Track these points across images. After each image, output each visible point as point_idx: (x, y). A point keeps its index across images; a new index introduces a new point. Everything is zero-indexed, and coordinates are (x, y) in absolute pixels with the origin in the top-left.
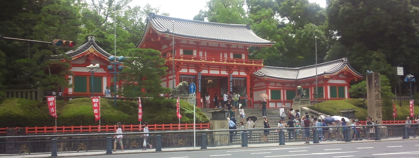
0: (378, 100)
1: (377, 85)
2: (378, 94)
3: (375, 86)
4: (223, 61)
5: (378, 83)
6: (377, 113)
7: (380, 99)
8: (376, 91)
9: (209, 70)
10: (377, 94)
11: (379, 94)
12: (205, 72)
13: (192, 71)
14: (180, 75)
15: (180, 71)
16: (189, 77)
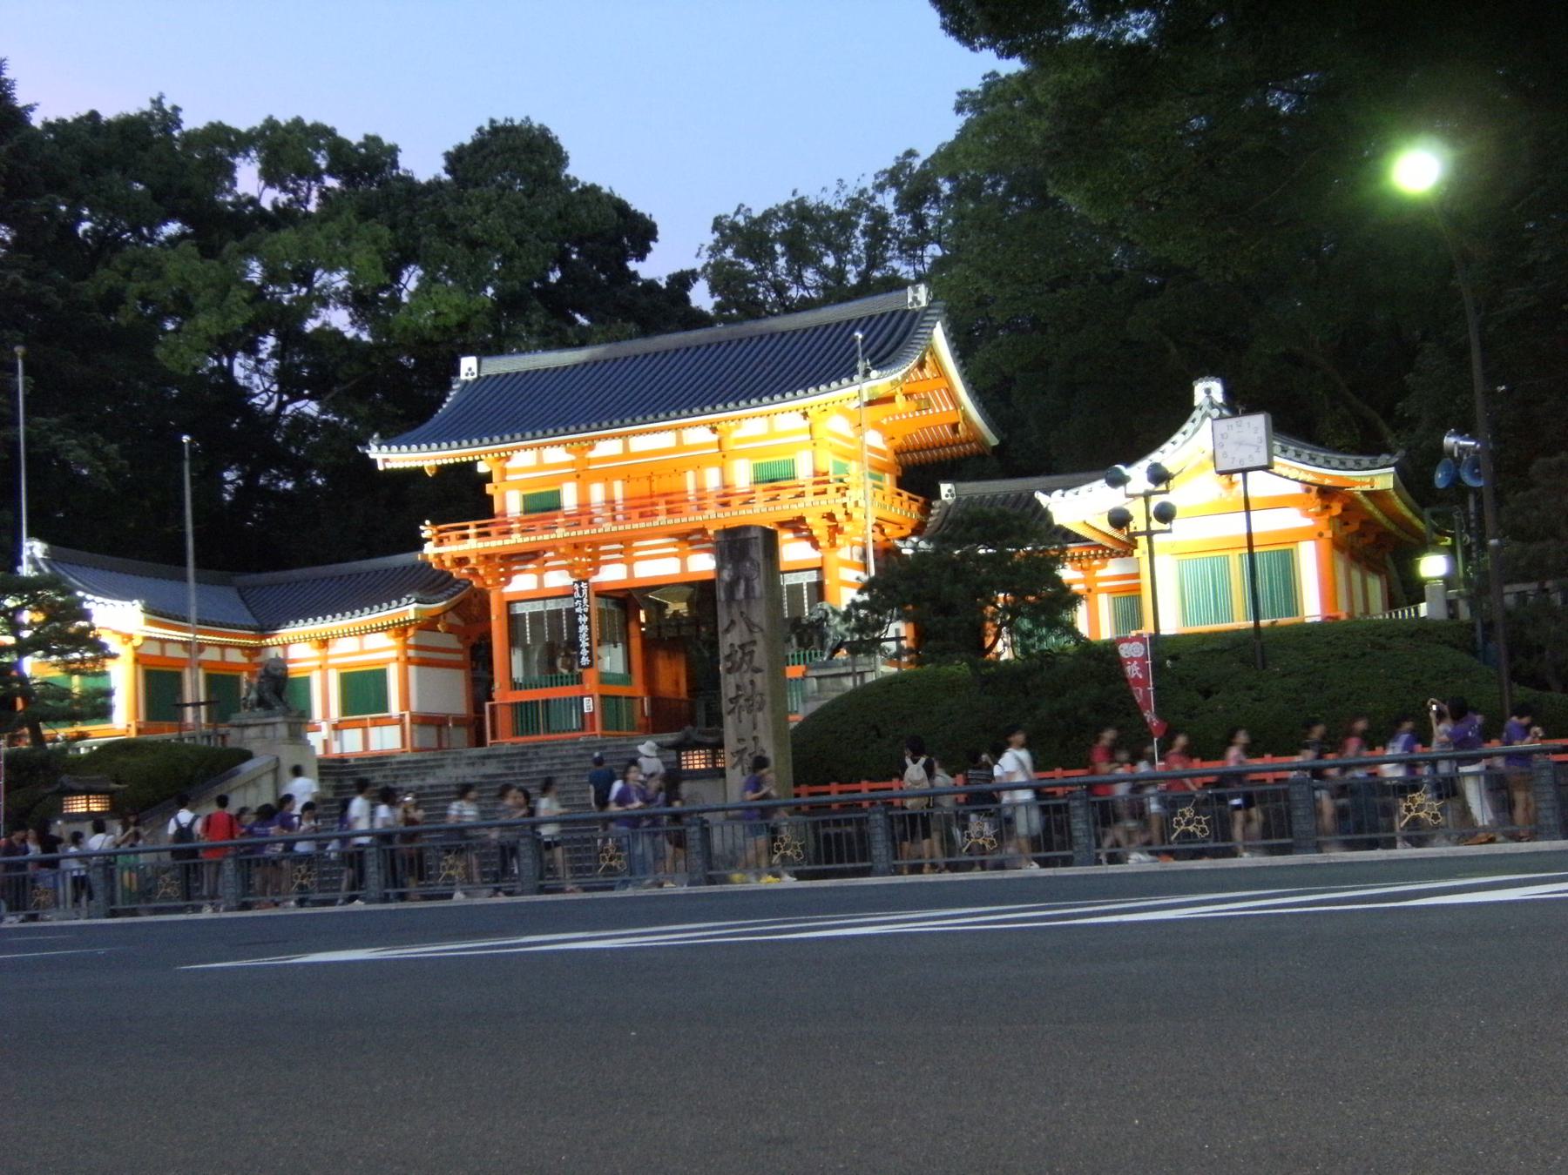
0: (747, 677)
1: (740, 594)
2: (747, 638)
3: (731, 597)
4: (701, 508)
5: (748, 581)
6: (741, 747)
7: (757, 670)
8: (733, 622)
9: (630, 563)
10: (737, 643)
11: (754, 643)
12: (612, 574)
13: (558, 579)
14: (509, 603)
15: (507, 589)
16: (552, 605)
